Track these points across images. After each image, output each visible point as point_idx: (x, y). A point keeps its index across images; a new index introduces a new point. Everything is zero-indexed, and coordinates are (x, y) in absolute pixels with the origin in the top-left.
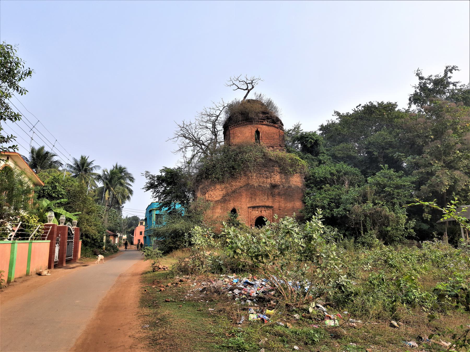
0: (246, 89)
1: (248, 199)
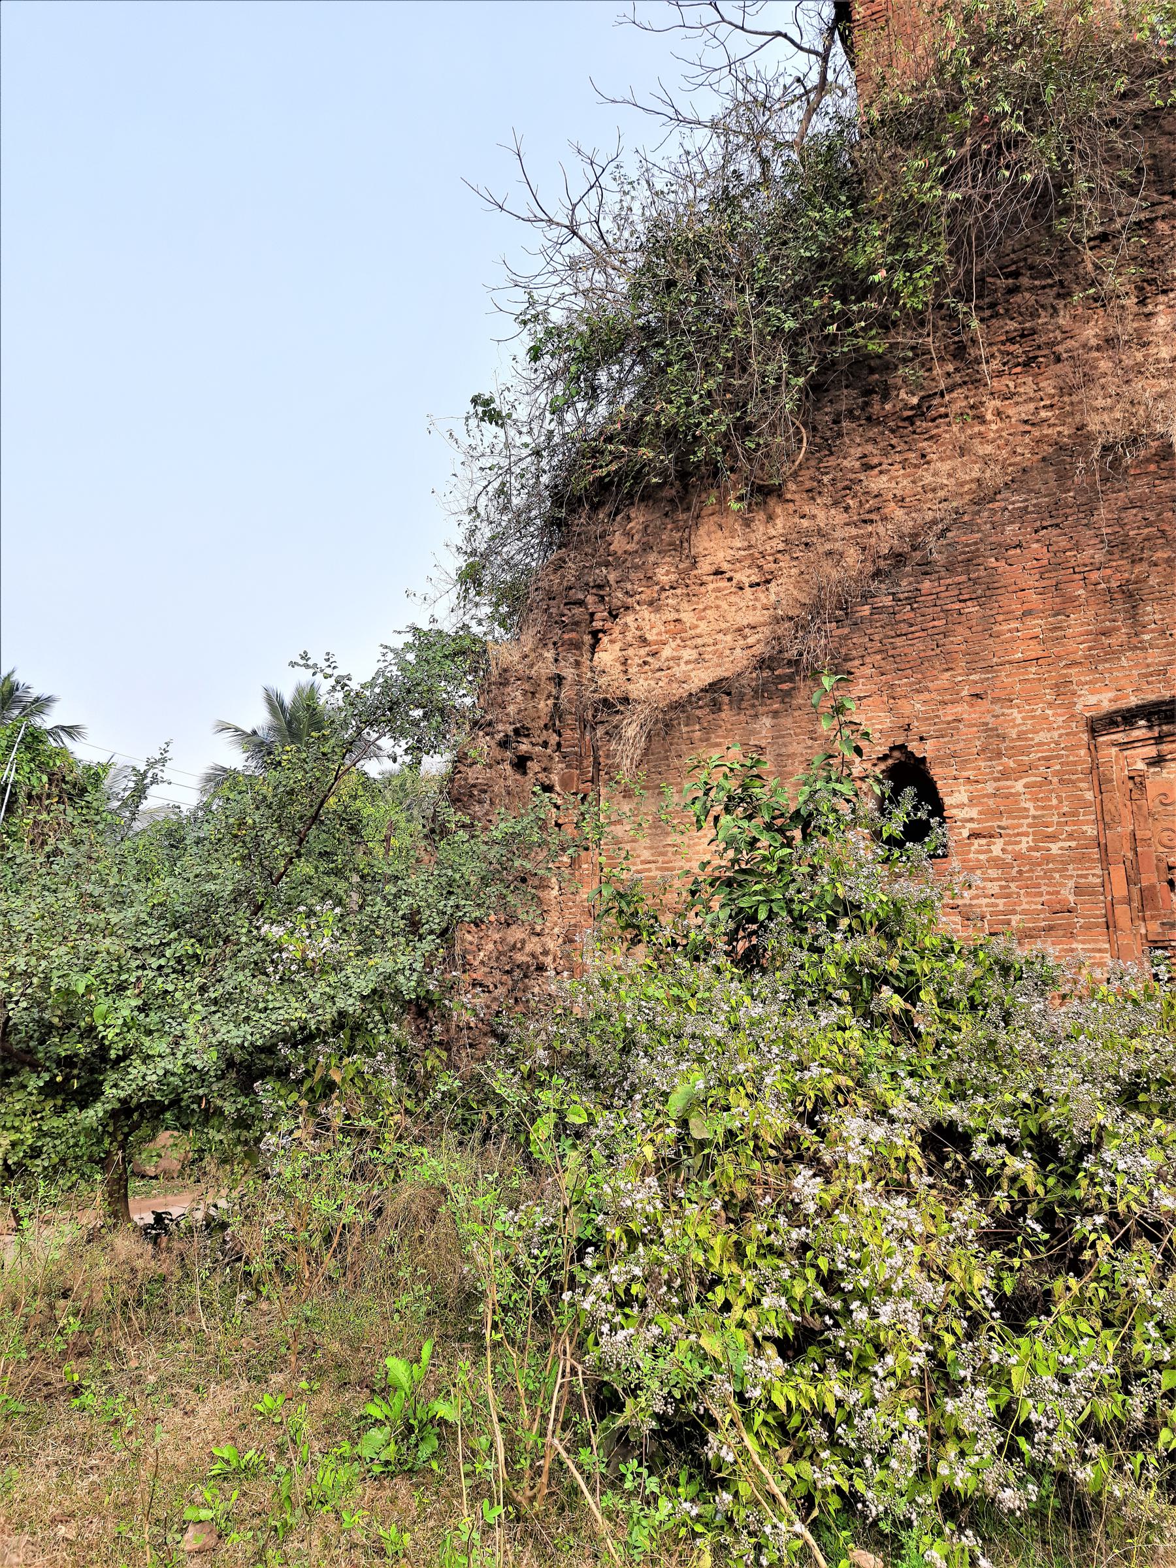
1: (1078, 623)
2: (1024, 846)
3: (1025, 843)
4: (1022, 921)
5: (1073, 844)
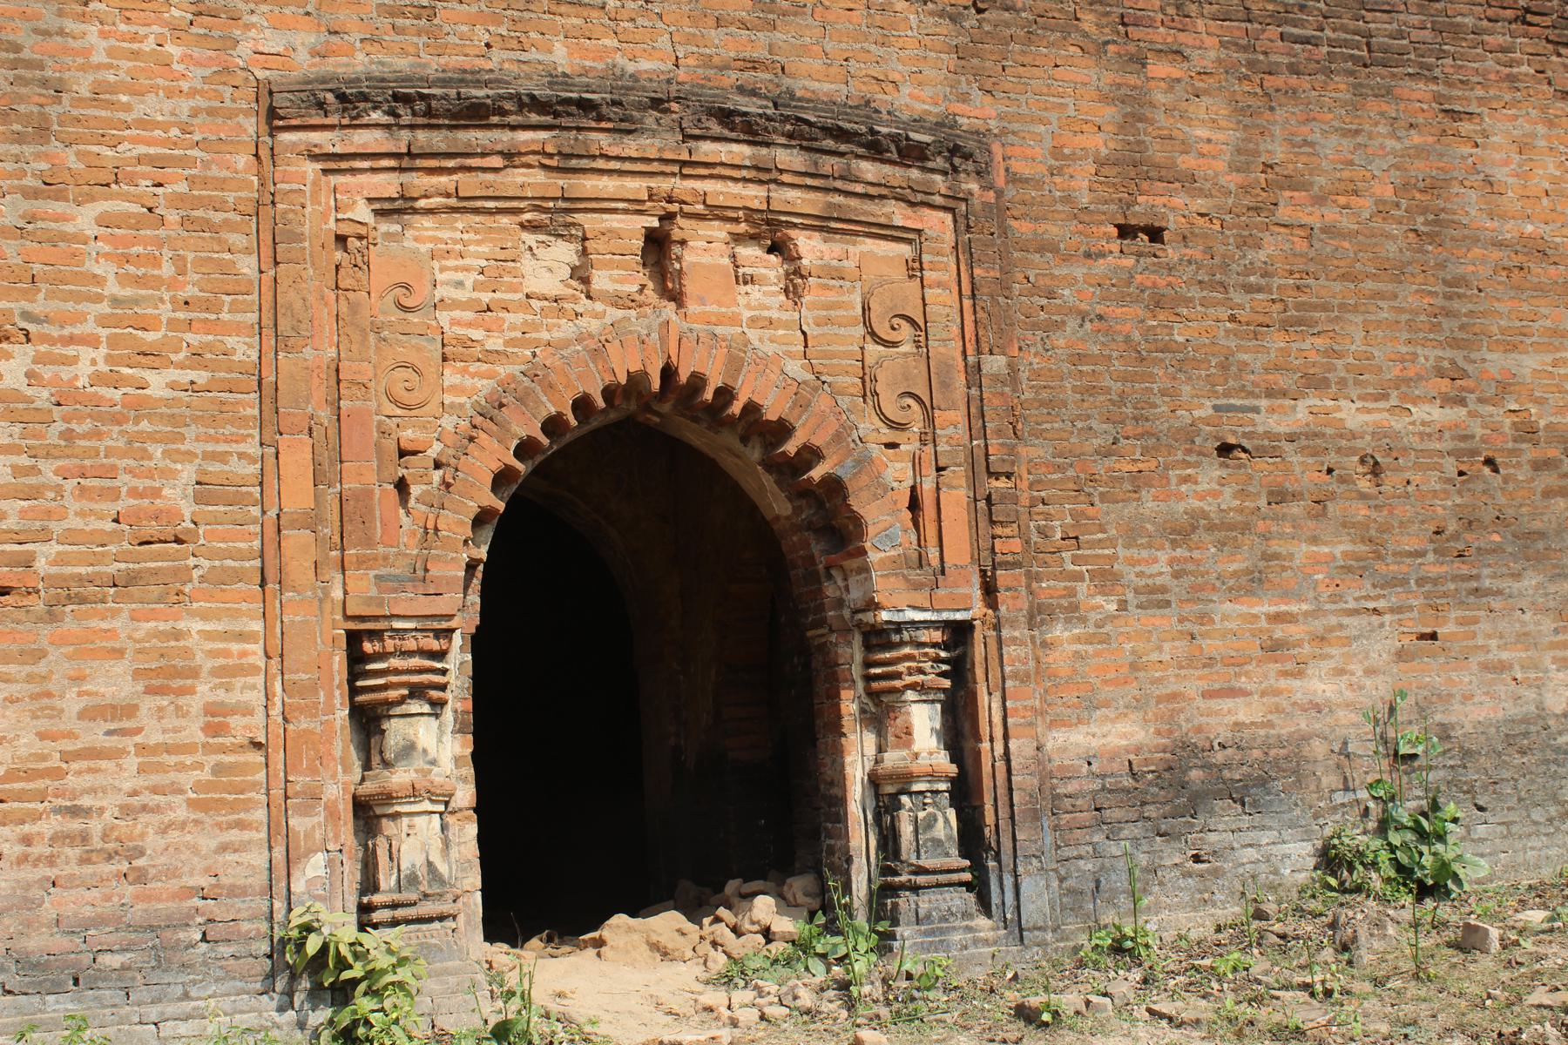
2: (83, 371)
3: (87, 363)
4: (60, 560)
5: (201, 377)
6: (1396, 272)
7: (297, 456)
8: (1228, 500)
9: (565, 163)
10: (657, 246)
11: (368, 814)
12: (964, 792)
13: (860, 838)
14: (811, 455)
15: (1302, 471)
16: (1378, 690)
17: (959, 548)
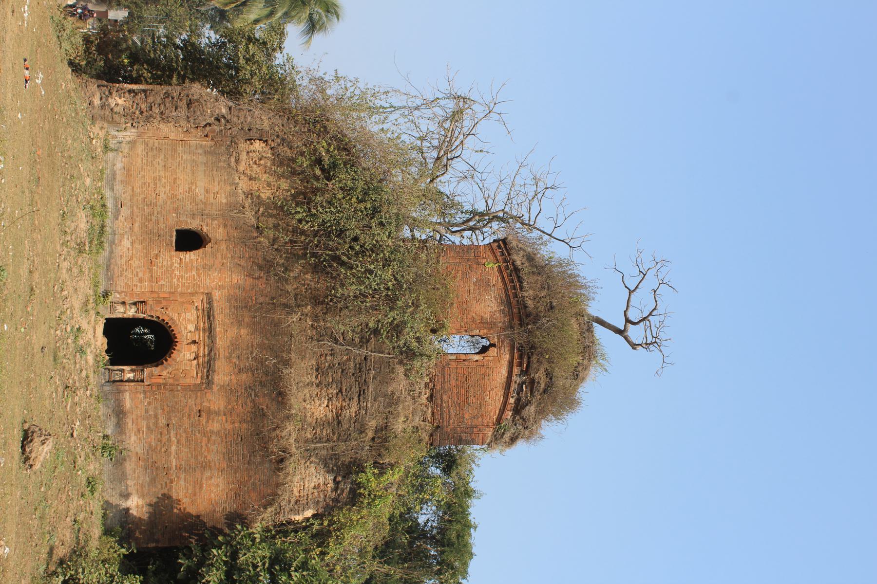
0: (628, 321)
3: (177, 273)
6: (196, 457)
7: (166, 296)
8: (161, 425)
9: (204, 330)
10: (194, 342)
11: (124, 303)
12: (122, 381)
13: (116, 368)
14: (166, 360)
15: (165, 438)
16: (132, 449)
17: (154, 381)
